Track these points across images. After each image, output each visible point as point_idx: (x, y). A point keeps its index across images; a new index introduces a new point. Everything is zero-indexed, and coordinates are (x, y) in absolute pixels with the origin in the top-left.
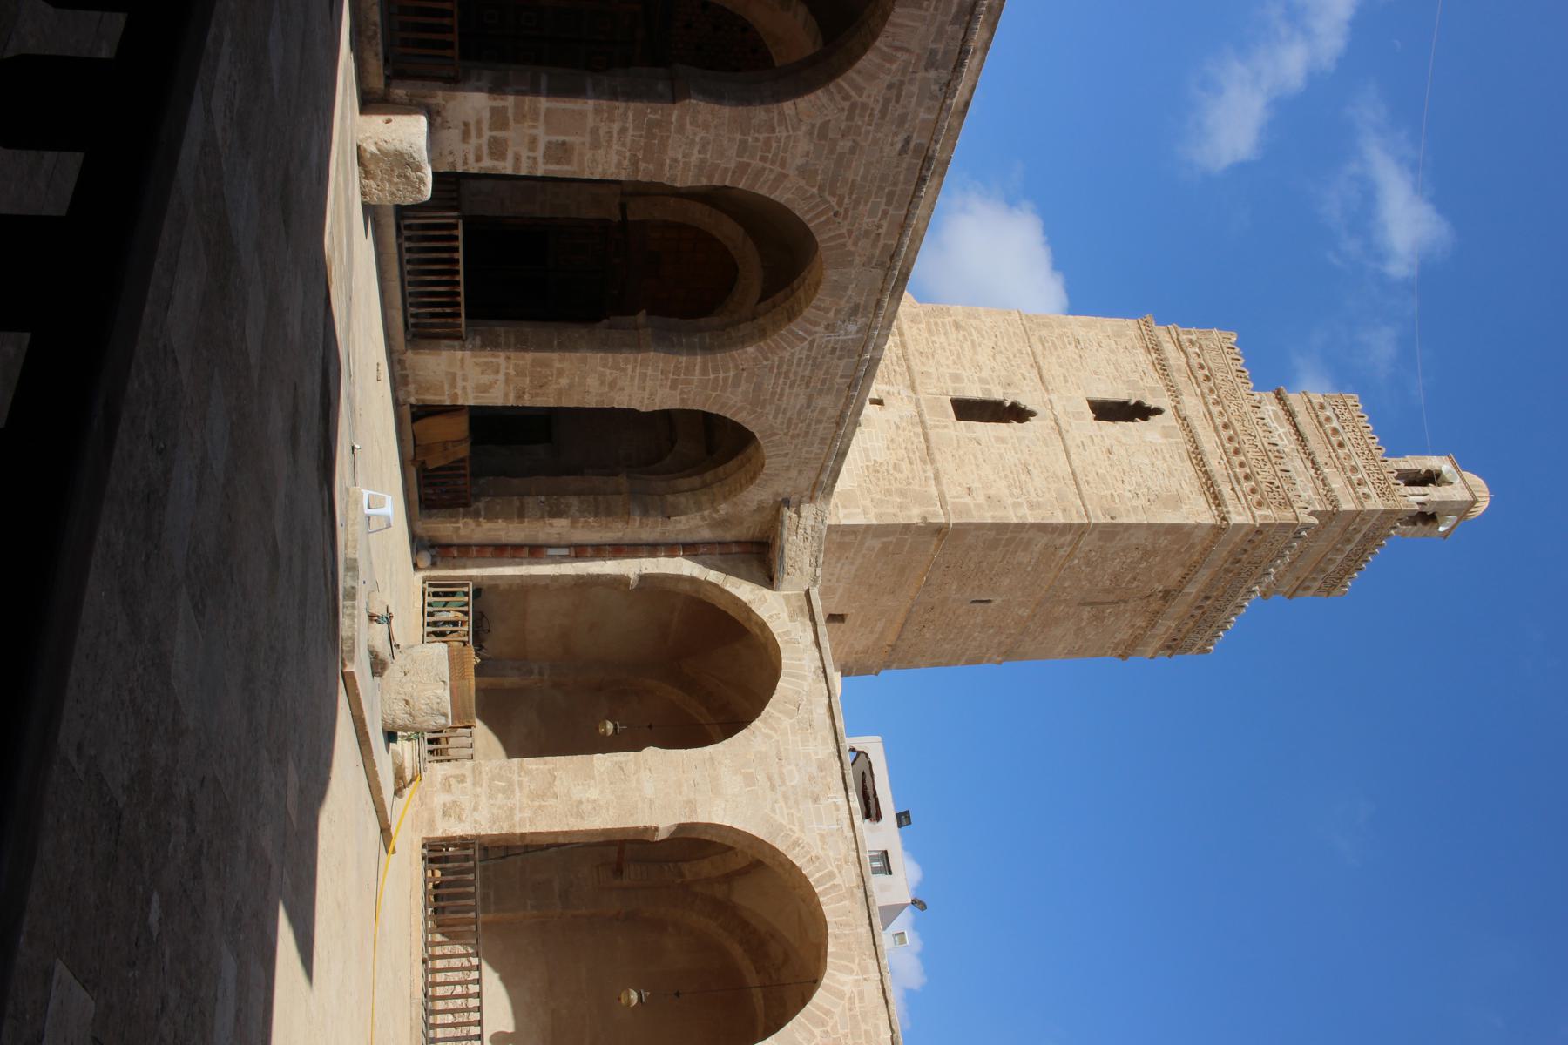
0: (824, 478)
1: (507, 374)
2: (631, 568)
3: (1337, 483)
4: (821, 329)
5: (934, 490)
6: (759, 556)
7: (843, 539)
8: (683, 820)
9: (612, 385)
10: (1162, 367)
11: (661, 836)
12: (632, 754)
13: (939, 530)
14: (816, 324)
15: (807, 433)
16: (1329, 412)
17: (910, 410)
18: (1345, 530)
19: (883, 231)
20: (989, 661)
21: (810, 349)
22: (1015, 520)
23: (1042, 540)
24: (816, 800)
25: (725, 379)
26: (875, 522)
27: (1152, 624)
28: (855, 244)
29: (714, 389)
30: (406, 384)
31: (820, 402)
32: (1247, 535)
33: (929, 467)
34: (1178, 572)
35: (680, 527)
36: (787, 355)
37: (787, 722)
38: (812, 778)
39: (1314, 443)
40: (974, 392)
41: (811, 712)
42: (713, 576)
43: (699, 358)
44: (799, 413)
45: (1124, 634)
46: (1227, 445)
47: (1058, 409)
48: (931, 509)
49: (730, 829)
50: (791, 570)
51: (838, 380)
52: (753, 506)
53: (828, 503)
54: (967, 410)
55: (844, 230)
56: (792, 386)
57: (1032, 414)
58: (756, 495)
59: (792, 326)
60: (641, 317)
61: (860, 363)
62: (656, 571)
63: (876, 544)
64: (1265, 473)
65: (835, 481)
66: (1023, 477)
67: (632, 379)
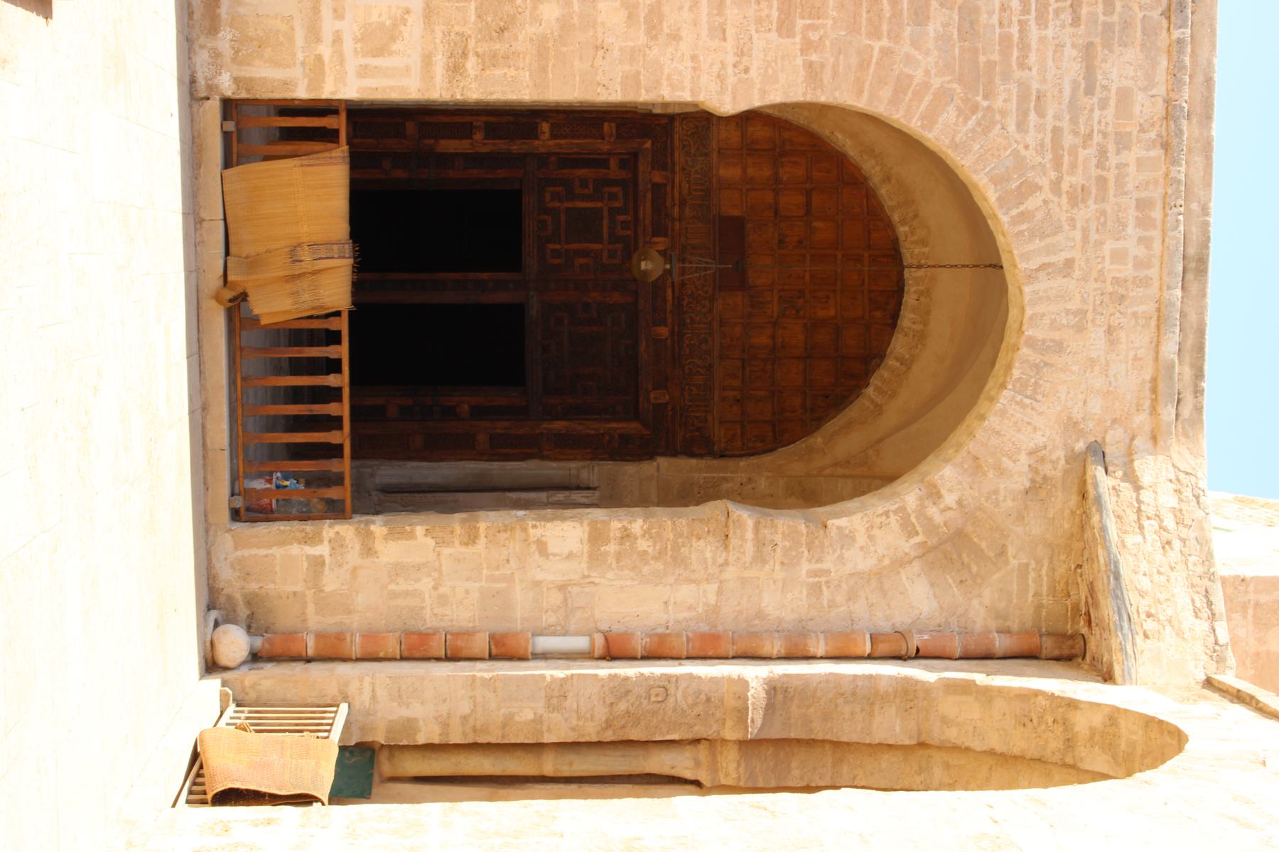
15: (1102, 181)
29: (875, 34)
30: (213, 30)
31: (1120, 68)
44: (1073, 106)
50: (1149, 625)
52: (1018, 475)
56: (1042, 20)
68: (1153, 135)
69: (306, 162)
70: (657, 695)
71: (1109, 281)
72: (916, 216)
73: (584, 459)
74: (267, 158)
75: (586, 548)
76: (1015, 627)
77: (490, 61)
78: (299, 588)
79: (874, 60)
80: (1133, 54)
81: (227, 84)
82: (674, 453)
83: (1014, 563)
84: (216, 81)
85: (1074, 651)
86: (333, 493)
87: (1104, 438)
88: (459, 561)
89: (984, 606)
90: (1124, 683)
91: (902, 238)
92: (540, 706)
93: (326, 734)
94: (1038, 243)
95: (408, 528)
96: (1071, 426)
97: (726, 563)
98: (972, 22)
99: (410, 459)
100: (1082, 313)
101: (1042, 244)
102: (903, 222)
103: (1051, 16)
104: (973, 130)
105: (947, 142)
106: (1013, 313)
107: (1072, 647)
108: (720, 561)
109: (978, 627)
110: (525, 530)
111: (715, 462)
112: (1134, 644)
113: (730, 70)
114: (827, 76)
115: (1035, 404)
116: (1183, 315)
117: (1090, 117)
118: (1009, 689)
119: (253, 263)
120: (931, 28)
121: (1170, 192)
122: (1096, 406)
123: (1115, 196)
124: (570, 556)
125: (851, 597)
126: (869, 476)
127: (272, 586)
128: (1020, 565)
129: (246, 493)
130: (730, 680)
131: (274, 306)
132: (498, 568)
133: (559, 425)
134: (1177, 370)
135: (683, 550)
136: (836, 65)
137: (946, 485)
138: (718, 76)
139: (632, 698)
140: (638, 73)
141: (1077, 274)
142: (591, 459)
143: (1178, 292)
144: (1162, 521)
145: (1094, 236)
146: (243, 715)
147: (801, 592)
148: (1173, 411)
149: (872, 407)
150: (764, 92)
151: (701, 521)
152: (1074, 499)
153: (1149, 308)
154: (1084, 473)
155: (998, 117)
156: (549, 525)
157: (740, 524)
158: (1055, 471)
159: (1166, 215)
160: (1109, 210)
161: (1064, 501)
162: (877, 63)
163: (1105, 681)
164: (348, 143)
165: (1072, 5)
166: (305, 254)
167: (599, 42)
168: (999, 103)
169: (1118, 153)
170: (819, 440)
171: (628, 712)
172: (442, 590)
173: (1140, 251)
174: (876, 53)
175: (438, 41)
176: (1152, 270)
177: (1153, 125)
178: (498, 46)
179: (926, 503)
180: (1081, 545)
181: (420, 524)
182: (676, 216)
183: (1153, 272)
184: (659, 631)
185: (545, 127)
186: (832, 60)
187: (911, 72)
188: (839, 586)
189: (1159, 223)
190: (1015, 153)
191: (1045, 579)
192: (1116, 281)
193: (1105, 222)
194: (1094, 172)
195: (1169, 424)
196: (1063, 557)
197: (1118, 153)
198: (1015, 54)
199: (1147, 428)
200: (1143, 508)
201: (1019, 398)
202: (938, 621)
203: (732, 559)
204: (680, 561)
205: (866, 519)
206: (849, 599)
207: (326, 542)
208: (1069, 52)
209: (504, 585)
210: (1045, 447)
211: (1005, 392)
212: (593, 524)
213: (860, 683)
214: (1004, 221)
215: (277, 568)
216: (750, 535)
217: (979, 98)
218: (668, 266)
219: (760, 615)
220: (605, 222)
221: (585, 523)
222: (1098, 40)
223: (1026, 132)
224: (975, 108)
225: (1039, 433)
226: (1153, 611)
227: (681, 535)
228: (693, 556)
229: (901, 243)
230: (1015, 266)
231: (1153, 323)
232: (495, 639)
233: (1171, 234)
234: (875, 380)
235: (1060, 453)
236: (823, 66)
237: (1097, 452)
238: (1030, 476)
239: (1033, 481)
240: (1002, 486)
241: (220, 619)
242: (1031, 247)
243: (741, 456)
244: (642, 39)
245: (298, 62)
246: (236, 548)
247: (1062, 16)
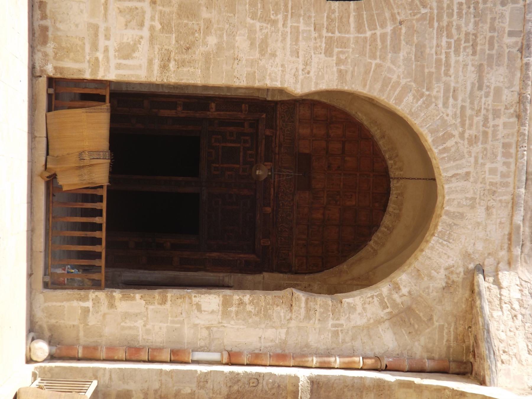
1: (152, 28)
15: (485, 133)
29: (374, 57)
30: (45, 42)
31: (496, 77)
44: (472, 95)
50: (504, 357)
67: (284, 40)
68: (512, 111)
69: (89, 111)
70: (253, 383)
71: (488, 183)
72: (397, 156)
73: (226, 272)
74: (70, 108)
75: (221, 309)
76: (437, 357)
77: (182, 63)
78: (76, 323)
79: (372, 70)
80: (503, 70)
81: (50, 70)
82: (272, 271)
83: (436, 324)
84: (45, 68)
85: (466, 370)
86: (96, 276)
87: (483, 263)
88: (157, 312)
89: (421, 345)
90: (490, 385)
91: (390, 166)
92: (194, 386)
93: (84, 393)
94: (452, 164)
95: (132, 295)
96: (467, 256)
97: (291, 319)
98: (422, 53)
99: (140, 268)
100: (473, 199)
101: (454, 164)
102: (390, 158)
103: (462, 50)
104: (421, 106)
105: (408, 111)
106: (439, 199)
107: (465, 368)
108: (288, 317)
109: (418, 356)
110: (190, 298)
111: (292, 276)
112: (496, 366)
113: (300, 72)
114: (348, 77)
115: (449, 244)
116: (526, 202)
117: (480, 102)
118: (431, 386)
119: (60, 159)
120: (402, 54)
121: (520, 139)
122: (480, 246)
123: (492, 141)
124: (213, 312)
125: (353, 339)
126: (366, 281)
127: (63, 321)
128: (439, 325)
129: (52, 275)
130: (290, 377)
131: (69, 182)
132: (176, 316)
133: (215, 255)
134: (522, 229)
135: (269, 311)
136: (353, 72)
137: (404, 283)
138: (294, 75)
139: (240, 384)
140: (255, 72)
141: (472, 179)
142: (230, 272)
143: (523, 190)
144: (512, 305)
145: (480, 161)
146: (43, 384)
147: (328, 335)
148: (520, 250)
149: (372, 251)
150: (317, 84)
151: (279, 297)
152: (467, 293)
153: (508, 198)
154: (473, 280)
155: (433, 100)
156: (202, 296)
157: (298, 299)
158: (459, 277)
159: (517, 151)
160: (488, 148)
161: (462, 294)
162: (374, 71)
163: (481, 384)
164: (110, 102)
165: (472, 45)
166: (86, 156)
167: (236, 56)
168: (434, 93)
169: (494, 119)
170: (345, 266)
171: (238, 391)
172: (148, 327)
173: (504, 169)
174: (373, 66)
175: (156, 53)
176: (510, 179)
177: (512, 106)
178: (185, 57)
179: (393, 292)
180: (470, 316)
181: (138, 293)
182: (277, 152)
183: (510, 180)
184: (257, 351)
185: (213, 105)
186: (351, 69)
187: (390, 76)
188: (348, 333)
189: (514, 155)
190: (442, 118)
191: (452, 333)
192: (491, 184)
193: (486, 154)
194: (481, 129)
195: (517, 256)
196: (461, 322)
197: (494, 119)
198: (443, 68)
199: (506, 258)
200: (503, 298)
201: (441, 241)
202: (397, 352)
203: (293, 317)
204: (268, 317)
205: (362, 299)
206: (353, 339)
207: (91, 300)
208: (470, 68)
209: (179, 325)
210: (453, 266)
211: (434, 238)
212: (224, 297)
213: (356, 381)
214: (435, 152)
215: (65, 313)
216: (303, 305)
217: (424, 90)
218: (270, 173)
219: (307, 346)
220: (241, 154)
221: (221, 296)
222: (485, 63)
223: (448, 108)
224: (422, 95)
225: (451, 259)
226: (506, 350)
227: (269, 304)
228: (275, 315)
229: (390, 169)
230: (440, 175)
231: (510, 205)
232: (173, 352)
233: (520, 161)
234: (374, 238)
235: (461, 270)
236: (346, 72)
237: (480, 269)
238: (445, 280)
239: (447, 283)
240: (431, 285)
241: (35, 337)
242: (448, 165)
243: (305, 274)
244: (257, 55)
245: (86, 61)
246: (45, 302)
247: (467, 50)
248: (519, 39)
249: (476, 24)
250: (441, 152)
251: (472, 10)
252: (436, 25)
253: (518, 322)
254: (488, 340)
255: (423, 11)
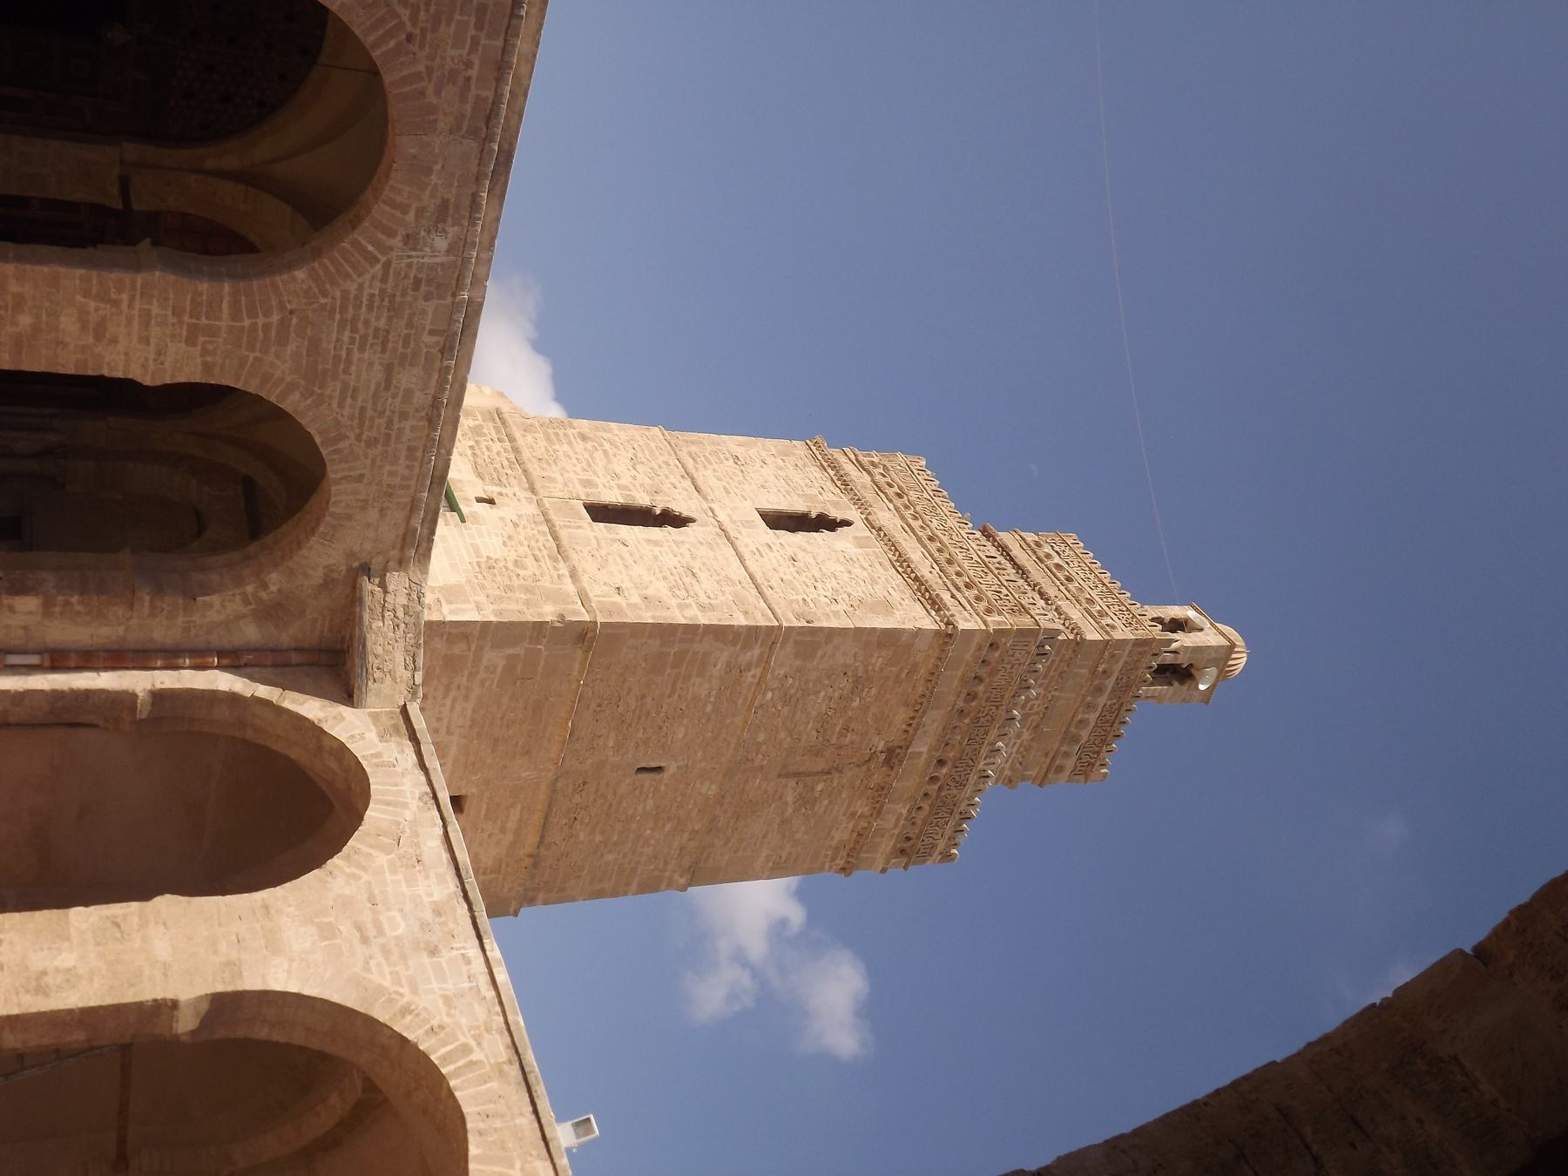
0: (416, 522)
2: (138, 682)
3: (1075, 614)
4: (396, 242)
5: (570, 587)
6: (335, 666)
7: (451, 647)
8: (220, 988)
9: (100, 331)
10: (845, 484)
11: (185, 1024)
12: (134, 905)
13: (582, 636)
14: (391, 233)
15: (388, 436)
16: (1047, 549)
17: (532, 509)
18: (1093, 672)
19: (473, 72)
20: (670, 885)
21: (384, 280)
22: (683, 621)
23: (722, 656)
24: (434, 952)
25: (267, 327)
26: (493, 618)
27: (878, 812)
28: (438, 93)
29: (253, 350)
31: (407, 378)
32: (980, 648)
33: (561, 564)
34: (901, 716)
35: (213, 616)
36: (353, 288)
37: (382, 859)
38: (425, 926)
39: (1036, 574)
40: (613, 497)
41: (418, 845)
42: (263, 691)
43: (227, 288)
44: (375, 396)
45: (842, 834)
46: (936, 555)
47: (722, 517)
48: (570, 607)
49: (299, 997)
50: (378, 674)
51: (427, 339)
52: (317, 576)
53: (425, 572)
54: (601, 513)
55: (422, 68)
56: (362, 349)
57: (693, 520)
58: (320, 556)
59: (357, 235)
60: (145, 244)
61: (455, 307)
62: (177, 686)
63: (495, 658)
64: (988, 584)
65: (433, 532)
66: (687, 580)
120: (290, 348)
145: (378, 463)
150: (173, 376)
153: (409, 500)
168: (328, 391)
173: (406, 472)
183: (413, 483)
190: (335, 419)
192: (389, 486)
208: (377, 366)
216: (147, 604)
224: (312, 394)
235: (344, 568)
244: (91, 340)
248: (441, 339)
249: (390, 319)
250: (330, 454)
251: (386, 303)
252: (338, 317)
253: (400, 633)
254: (364, 655)
255: (322, 301)
